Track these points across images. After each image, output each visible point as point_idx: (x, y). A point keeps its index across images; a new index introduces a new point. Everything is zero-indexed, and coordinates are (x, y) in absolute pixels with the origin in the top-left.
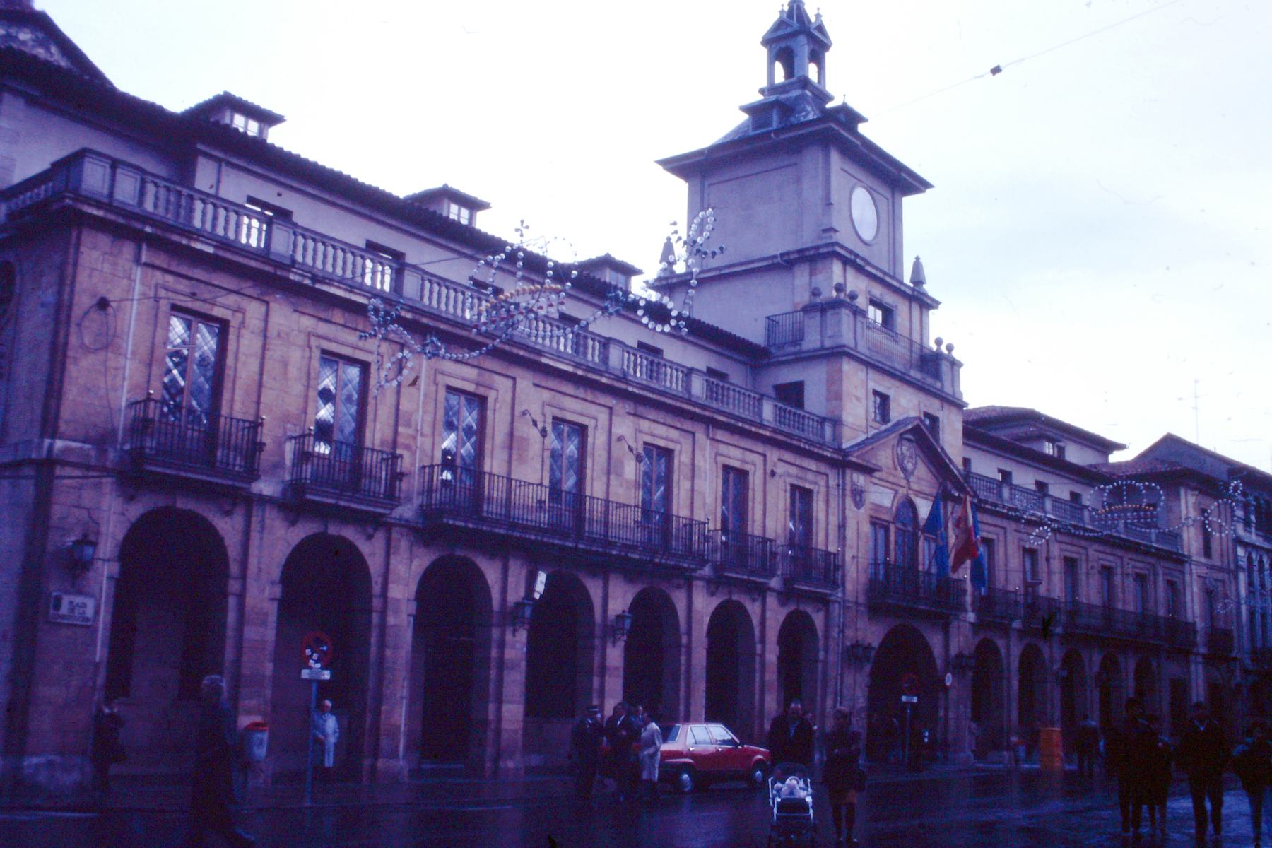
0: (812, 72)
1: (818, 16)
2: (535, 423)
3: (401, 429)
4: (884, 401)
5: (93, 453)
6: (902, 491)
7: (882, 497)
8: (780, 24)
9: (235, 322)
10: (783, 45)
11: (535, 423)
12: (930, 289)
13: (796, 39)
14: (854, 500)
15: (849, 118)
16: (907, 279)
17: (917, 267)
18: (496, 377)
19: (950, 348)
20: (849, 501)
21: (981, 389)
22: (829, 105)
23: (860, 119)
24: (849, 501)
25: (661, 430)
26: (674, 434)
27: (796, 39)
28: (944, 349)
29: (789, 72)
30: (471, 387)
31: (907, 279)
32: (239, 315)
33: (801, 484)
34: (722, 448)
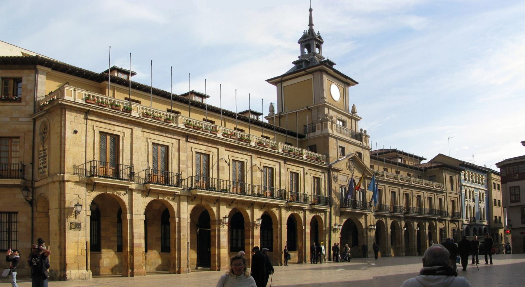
4: (343, 149)
12: (359, 114)
19: (365, 132)
33: (316, 176)
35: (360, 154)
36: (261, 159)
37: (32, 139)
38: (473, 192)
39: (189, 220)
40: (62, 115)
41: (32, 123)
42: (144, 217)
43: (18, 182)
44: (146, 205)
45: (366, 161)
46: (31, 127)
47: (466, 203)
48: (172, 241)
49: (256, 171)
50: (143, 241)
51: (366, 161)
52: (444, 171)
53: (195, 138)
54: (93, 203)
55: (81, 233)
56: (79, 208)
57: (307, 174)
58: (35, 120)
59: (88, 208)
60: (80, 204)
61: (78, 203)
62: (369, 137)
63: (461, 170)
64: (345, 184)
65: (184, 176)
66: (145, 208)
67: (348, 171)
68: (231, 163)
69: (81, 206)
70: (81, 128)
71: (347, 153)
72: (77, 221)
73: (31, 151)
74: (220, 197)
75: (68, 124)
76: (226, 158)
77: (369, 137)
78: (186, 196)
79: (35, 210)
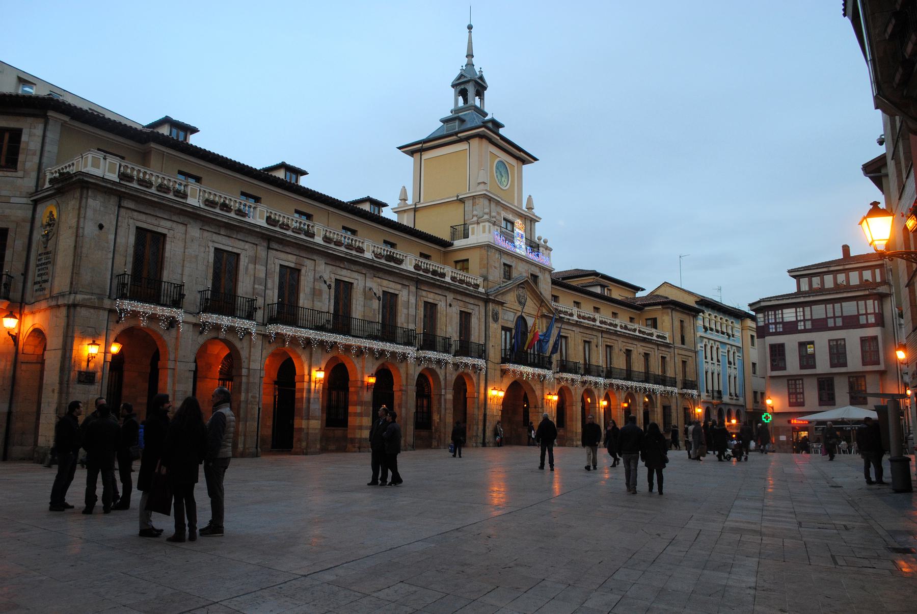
1: (481, 71)
2: (325, 282)
7: (509, 319)
8: (461, 76)
9: (169, 234)
10: (462, 87)
11: (325, 282)
12: (537, 211)
13: (470, 85)
14: (493, 318)
16: (524, 208)
19: (545, 242)
21: (561, 261)
22: (487, 118)
23: (502, 126)
25: (392, 285)
26: (399, 287)
30: (292, 265)
31: (524, 208)
33: (466, 310)
34: (424, 293)
35: (535, 277)
36: (379, 280)
37: (28, 233)
40: (81, 198)
41: (31, 207)
45: (545, 287)
46: (30, 213)
47: (705, 365)
49: (371, 299)
51: (545, 287)
57: (450, 305)
58: (36, 203)
62: (551, 250)
64: (511, 325)
65: (260, 302)
67: (517, 303)
68: (333, 285)
70: (109, 221)
71: (515, 274)
73: (25, 254)
75: (90, 213)
76: (326, 277)
77: (551, 250)
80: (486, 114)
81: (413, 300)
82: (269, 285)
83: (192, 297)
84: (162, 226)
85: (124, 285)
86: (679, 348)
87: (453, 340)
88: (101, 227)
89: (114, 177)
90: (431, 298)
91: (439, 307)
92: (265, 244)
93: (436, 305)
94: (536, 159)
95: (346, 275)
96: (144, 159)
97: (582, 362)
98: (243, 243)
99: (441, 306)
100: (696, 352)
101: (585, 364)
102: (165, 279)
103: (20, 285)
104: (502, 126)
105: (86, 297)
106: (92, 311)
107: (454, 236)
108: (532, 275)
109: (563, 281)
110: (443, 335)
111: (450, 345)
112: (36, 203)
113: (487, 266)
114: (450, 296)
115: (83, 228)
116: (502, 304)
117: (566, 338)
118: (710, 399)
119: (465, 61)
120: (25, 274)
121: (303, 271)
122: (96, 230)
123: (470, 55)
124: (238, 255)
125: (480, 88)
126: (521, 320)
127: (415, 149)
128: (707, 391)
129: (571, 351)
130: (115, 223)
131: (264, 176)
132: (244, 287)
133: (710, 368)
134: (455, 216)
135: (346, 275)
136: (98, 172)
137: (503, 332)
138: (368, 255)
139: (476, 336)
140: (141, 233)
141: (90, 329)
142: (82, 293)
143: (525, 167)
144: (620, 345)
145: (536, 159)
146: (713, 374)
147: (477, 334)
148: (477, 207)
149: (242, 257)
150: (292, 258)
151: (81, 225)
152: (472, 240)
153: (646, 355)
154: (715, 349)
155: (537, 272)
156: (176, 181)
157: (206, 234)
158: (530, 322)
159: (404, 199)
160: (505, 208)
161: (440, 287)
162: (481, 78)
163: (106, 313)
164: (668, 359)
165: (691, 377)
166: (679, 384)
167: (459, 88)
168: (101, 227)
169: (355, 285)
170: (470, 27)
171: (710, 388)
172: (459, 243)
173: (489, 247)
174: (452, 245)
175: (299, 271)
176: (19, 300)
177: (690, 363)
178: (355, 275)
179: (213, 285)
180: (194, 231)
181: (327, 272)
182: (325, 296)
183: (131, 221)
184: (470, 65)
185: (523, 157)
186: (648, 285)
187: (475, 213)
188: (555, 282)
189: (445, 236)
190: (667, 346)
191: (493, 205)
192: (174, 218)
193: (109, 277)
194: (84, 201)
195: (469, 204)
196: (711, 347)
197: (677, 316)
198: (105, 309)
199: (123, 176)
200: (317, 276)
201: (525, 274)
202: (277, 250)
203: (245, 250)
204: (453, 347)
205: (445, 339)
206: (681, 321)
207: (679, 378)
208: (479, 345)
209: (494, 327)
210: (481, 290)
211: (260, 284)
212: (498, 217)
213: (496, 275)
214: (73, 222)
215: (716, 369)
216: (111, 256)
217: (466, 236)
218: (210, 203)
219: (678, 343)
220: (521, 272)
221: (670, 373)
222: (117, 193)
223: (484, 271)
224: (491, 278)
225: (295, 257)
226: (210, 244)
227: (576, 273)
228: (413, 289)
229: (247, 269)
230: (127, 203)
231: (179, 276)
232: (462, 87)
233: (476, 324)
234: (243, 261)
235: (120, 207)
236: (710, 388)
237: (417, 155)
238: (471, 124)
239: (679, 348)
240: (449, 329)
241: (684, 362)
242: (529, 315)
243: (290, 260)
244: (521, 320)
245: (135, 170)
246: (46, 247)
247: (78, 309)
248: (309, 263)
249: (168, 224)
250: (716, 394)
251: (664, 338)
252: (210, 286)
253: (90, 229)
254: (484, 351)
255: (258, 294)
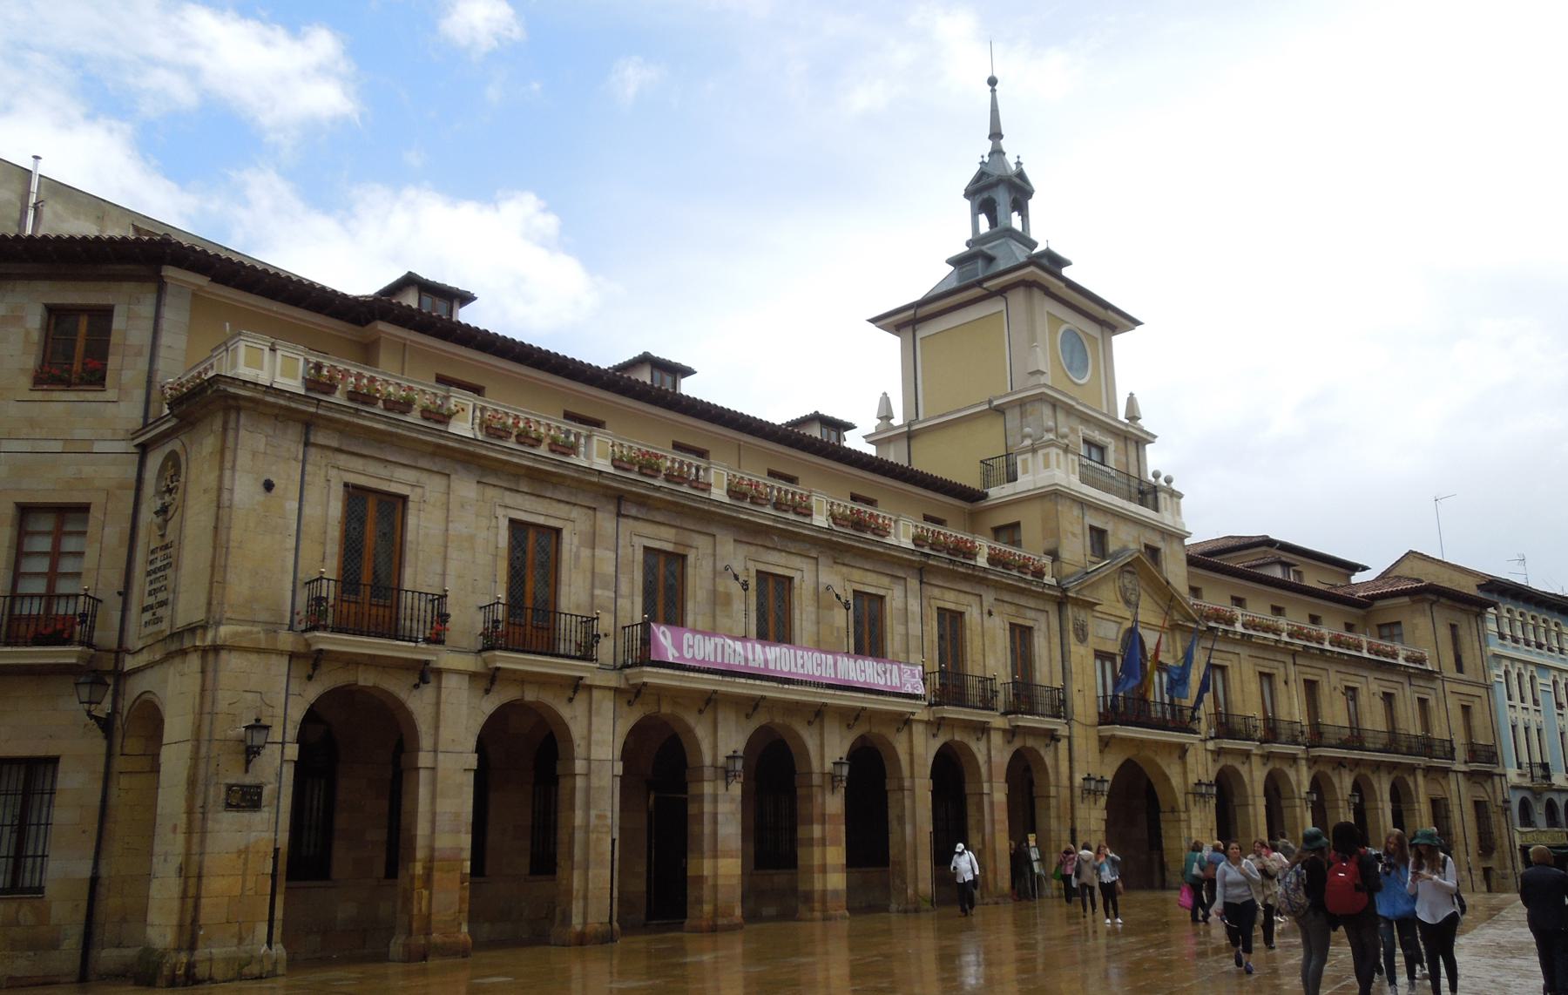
0: (1016, 221)
1: (1019, 164)
2: (736, 577)
3: (597, 592)
4: (1099, 535)
5: (262, 635)
6: (1128, 624)
7: (1108, 634)
8: (981, 175)
9: (414, 495)
11: (736, 577)
12: (1147, 423)
13: (1000, 190)
14: (1077, 635)
15: (1053, 262)
16: (1121, 416)
17: (1131, 400)
18: (695, 536)
19: (1169, 480)
20: (1072, 638)
21: (1207, 516)
22: (1036, 251)
23: (1066, 263)
24: (1072, 638)
25: (871, 578)
26: (886, 581)
27: (1000, 190)
28: (1162, 481)
29: (993, 221)
30: (669, 547)
31: (1121, 416)
32: (419, 490)
33: (1020, 621)
34: (936, 592)
35: (1153, 552)
36: (845, 569)
38: (1532, 678)
39: (619, 768)
40: (225, 429)
41: (136, 458)
42: (472, 761)
43: (67, 655)
44: (482, 720)
45: (1176, 572)
46: (132, 472)
47: (1510, 713)
48: (562, 835)
49: (830, 607)
50: (466, 840)
51: (1176, 572)
52: (1427, 606)
53: (642, 501)
54: (312, 716)
55: (262, 818)
56: (258, 738)
57: (990, 613)
58: (144, 449)
59: (292, 733)
60: (265, 722)
61: (258, 720)
62: (1180, 496)
63: (1483, 605)
64: (1114, 647)
65: (605, 624)
66: (476, 729)
67: (1121, 605)
68: (753, 583)
69: (267, 728)
70: (286, 476)
71: (1112, 547)
72: (248, 780)
73: (124, 551)
74: (715, 692)
75: (244, 458)
76: (738, 567)
77: (1180, 496)
78: (610, 688)
79: (117, 749)
80: (1035, 244)
81: (914, 606)
82: (624, 588)
83: (466, 619)
84: (397, 480)
85: (319, 600)
86: (1455, 681)
87: (999, 681)
88: (269, 486)
89: (295, 385)
90: (950, 600)
91: (967, 617)
92: (612, 508)
93: (961, 614)
94: (1137, 323)
95: (778, 562)
96: (367, 353)
97: (1259, 714)
98: (567, 508)
99: (973, 615)
100: (1488, 688)
101: (1266, 719)
102: (408, 584)
103: (117, 615)
104: (1066, 263)
105: (240, 629)
106: (254, 657)
107: (988, 478)
108: (1146, 546)
109: (1216, 560)
110: (978, 673)
111: (995, 693)
112: (144, 449)
113: (1054, 532)
114: (989, 597)
115: (231, 491)
116: (1091, 606)
117: (1223, 668)
118: (1526, 782)
119: (988, 145)
120: (125, 594)
121: (691, 559)
122: (260, 495)
123: (996, 135)
124: (558, 531)
125: (1019, 191)
126: (1132, 639)
127: (904, 322)
128: (1520, 766)
129: (1235, 696)
130: (298, 478)
131: (617, 381)
132: (573, 595)
133: (1521, 717)
134: (989, 440)
135: (778, 562)
136: (264, 378)
137: (1098, 663)
138: (820, 520)
139: (1045, 672)
140: (356, 495)
141: (249, 696)
142: (230, 621)
143: (1118, 341)
144: (1332, 681)
145: (1137, 323)
146: (1527, 729)
147: (1045, 669)
148: (1030, 419)
149: (565, 534)
150: (669, 533)
151: (227, 483)
152: (1026, 482)
153: (1388, 698)
154: (1527, 678)
155: (1157, 541)
156: (426, 393)
157: (490, 492)
158: (1150, 638)
159: (886, 416)
160: (1086, 419)
161: (966, 578)
162: (1021, 175)
163: (285, 661)
164: (1432, 702)
165: (1481, 739)
166: (1461, 753)
167: (979, 198)
168: (269, 486)
169: (797, 581)
170: (992, 82)
171: (1525, 759)
172: (997, 493)
173: (1055, 495)
174: (985, 496)
175: (684, 557)
176: (115, 646)
177: (1477, 708)
178: (797, 562)
179: (511, 592)
180: (466, 488)
181: (738, 558)
182: (738, 606)
183: (333, 473)
184: (997, 152)
185: (1111, 320)
186: (1374, 557)
187: (1027, 430)
188: (1192, 561)
189: (972, 480)
190: (1430, 675)
191: (1061, 417)
192: (423, 463)
193: (289, 586)
194: (231, 434)
195: (1013, 417)
196: (1520, 675)
197: (1443, 618)
198: (281, 653)
199: (312, 384)
200: (720, 566)
201: (1133, 546)
202: (636, 518)
203: (575, 525)
204: (1001, 696)
205: (984, 680)
206: (1453, 627)
207: (1459, 741)
208: (1053, 689)
209: (1081, 654)
210: (1048, 579)
211: (604, 588)
212: (1072, 437)
213: (1075, 550)
214: (211, 479)
215: (1534, 720)
216: (291, 543)
217: (1012, 478)
218: (494, 431)
219: (1450, 670)
220: (1123, 539)
221: (1439, 732)
222: (302, 417)
223: (1050, 545)
224: (1065, 554)
225: (673, 531)
226: (500, 512)
227: (1232, 543)
228: (913, 583)
229: (577, 557)
230: (320, 437)
231: (437, 580)
232: (985, 195)
233: (1043, 648)
234: (569, 543)
235: (307, 444)
236: (1525, 759)
237: (909, 331)
238: (1005, 280)
239: (1455, 681)
240: (991, 661)
241: (1466, 710)
242: (1148, 626)
243: (664, 538)
244: (1132, 639)
245: (351, 372)
246: (163, 536)
247: (224, 655)
248: (702, 542)
249: (411, 475)
250: (1538, 772)
251: (1421, 661)
252: (502, 595)
253: (244, 489)
254: (1064, 702)
255: (601, 608)
